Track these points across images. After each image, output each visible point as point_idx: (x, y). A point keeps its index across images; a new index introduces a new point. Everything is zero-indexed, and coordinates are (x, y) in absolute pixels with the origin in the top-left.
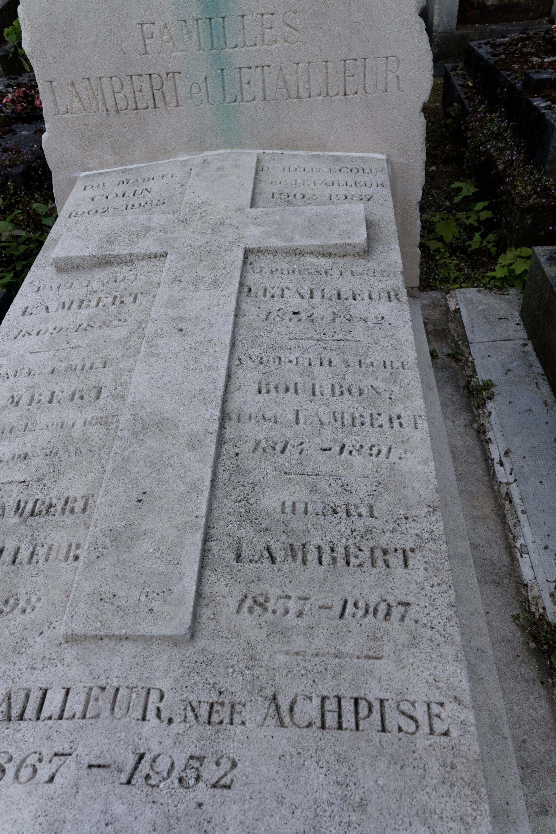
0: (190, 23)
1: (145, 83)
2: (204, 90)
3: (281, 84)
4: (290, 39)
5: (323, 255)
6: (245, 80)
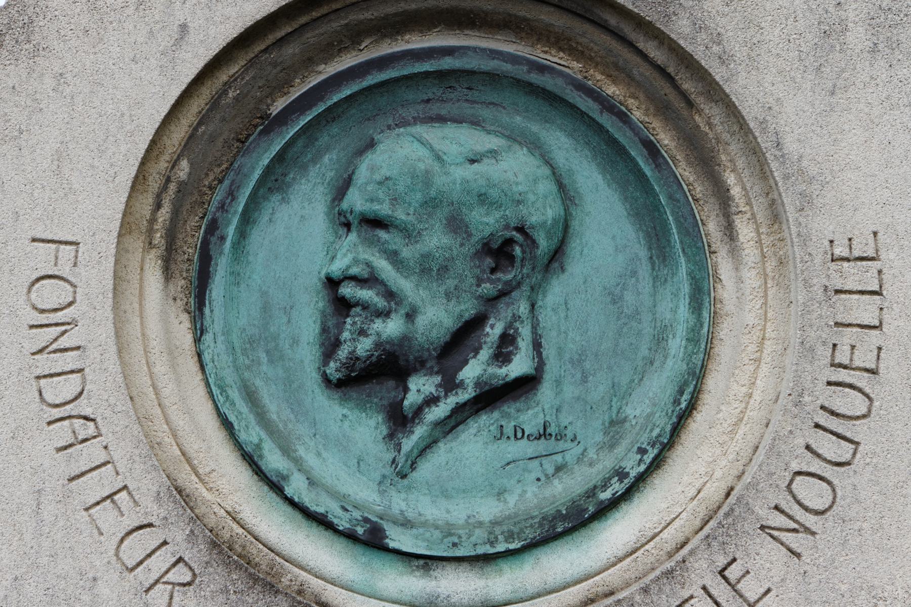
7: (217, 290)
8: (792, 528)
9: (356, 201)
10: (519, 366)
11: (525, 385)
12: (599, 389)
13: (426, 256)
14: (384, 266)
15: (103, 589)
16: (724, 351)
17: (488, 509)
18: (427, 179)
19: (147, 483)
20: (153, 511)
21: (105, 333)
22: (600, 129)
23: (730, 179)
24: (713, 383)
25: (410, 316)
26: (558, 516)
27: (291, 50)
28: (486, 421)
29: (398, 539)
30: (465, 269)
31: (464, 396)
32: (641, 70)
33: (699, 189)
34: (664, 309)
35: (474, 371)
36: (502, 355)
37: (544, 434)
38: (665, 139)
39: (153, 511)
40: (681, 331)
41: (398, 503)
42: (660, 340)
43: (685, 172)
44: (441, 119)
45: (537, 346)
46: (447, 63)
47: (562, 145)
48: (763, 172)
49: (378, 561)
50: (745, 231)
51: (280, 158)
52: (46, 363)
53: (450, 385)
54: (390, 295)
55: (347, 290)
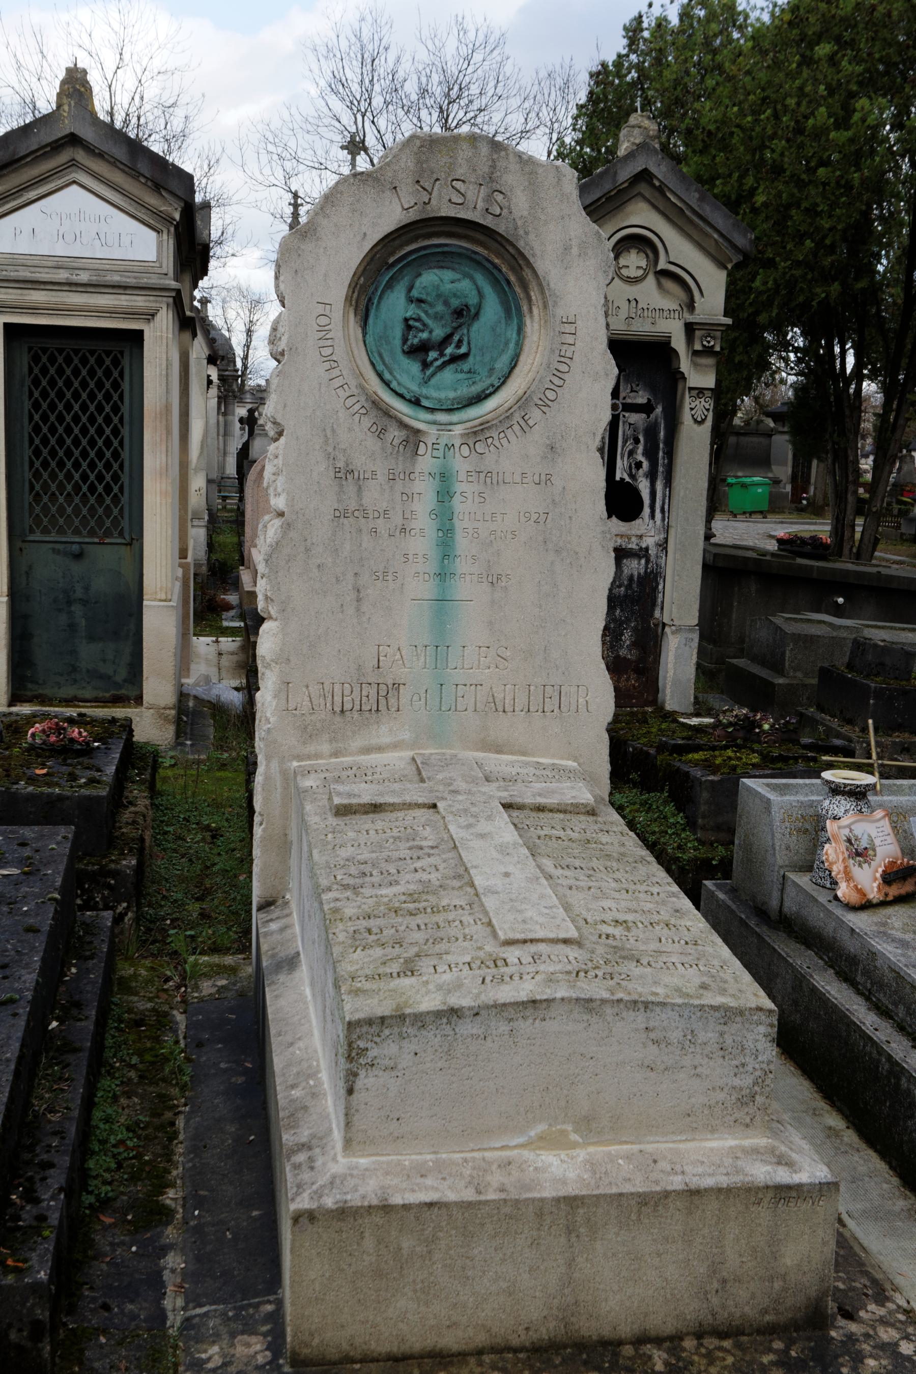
0: (419, 648)
1: (373, 692)
2: (423, 700)
3: (491, 699)
4: (501, 667)
5: (561, 812)
6: (460, 694)
7: (371, 320)
8: (544, 405)
9: (415, 293)
10: (463, 350)
11: (465, 356)
12: (487, 358)
13: (437, 313)
14: (423, 315)
15: (340, 415)
16: (526, 348)
17: (452, 395)
18: (438, 287)
19: (353, 383)
20: (355, 391)
21: (340, 334)
22: (492, 274)
23: (532, 294)
24: (522, 358)
25: (431, 332)
26: (473, 398)
27: (397, 242)
28: (452, 367)
29: (425, 403)
30: (448, 318)
31: (446, 358)
32: (507, 256)
33: (522, 296)
34: (509, 334)
35: (449, 351)
36: (458, 346)
37: (470, 372)
38: (512, 278)
39: (355, 391)
40: (513, 341)
41: (424, 391)
42: (507, 344)
43: (518, 289)
44: (442, 267)
45: (469, 343)
46: (446, 249)
47: (480, 278)
48: (542, 292)
49: (418, 409)
50: (535, 311)
51: (391, 278)
52: (322, 343)
53: (442, 355)
54: (424, 325)
55: (411, 322)
